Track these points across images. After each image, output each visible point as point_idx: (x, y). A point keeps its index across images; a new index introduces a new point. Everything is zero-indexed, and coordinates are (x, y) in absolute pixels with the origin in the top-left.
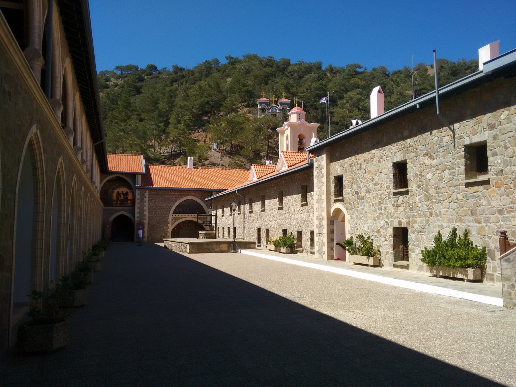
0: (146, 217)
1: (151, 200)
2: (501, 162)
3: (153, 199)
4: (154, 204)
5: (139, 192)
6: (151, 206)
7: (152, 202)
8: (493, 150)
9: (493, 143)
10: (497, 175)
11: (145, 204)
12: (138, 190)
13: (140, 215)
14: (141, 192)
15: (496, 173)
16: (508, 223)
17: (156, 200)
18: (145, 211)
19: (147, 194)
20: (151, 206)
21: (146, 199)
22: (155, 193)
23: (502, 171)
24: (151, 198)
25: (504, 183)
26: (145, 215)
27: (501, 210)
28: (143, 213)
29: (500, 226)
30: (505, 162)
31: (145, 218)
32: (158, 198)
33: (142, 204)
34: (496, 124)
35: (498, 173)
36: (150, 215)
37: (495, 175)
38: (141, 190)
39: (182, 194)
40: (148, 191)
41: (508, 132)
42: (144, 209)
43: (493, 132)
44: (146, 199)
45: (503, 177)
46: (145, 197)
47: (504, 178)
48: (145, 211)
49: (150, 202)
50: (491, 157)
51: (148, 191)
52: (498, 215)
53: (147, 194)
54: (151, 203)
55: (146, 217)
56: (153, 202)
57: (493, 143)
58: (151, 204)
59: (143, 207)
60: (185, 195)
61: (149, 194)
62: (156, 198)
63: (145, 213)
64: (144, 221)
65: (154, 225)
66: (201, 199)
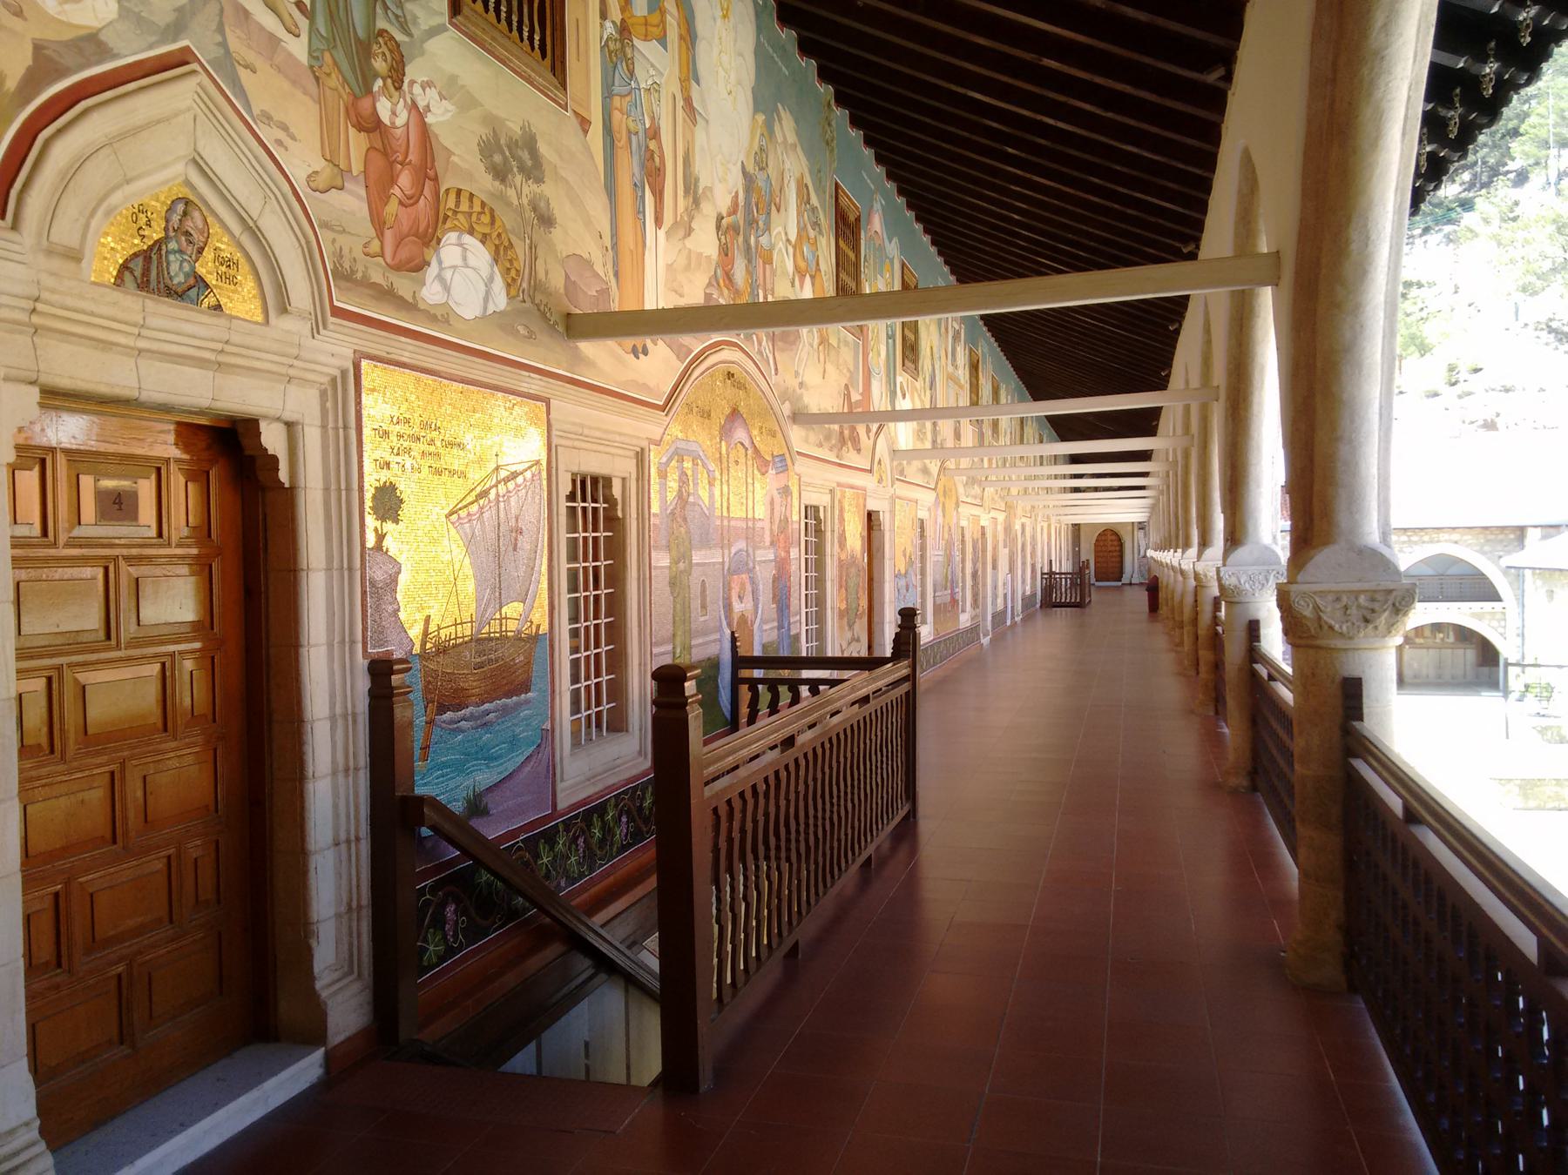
39: (1415, 538)
60: (1424, 542)
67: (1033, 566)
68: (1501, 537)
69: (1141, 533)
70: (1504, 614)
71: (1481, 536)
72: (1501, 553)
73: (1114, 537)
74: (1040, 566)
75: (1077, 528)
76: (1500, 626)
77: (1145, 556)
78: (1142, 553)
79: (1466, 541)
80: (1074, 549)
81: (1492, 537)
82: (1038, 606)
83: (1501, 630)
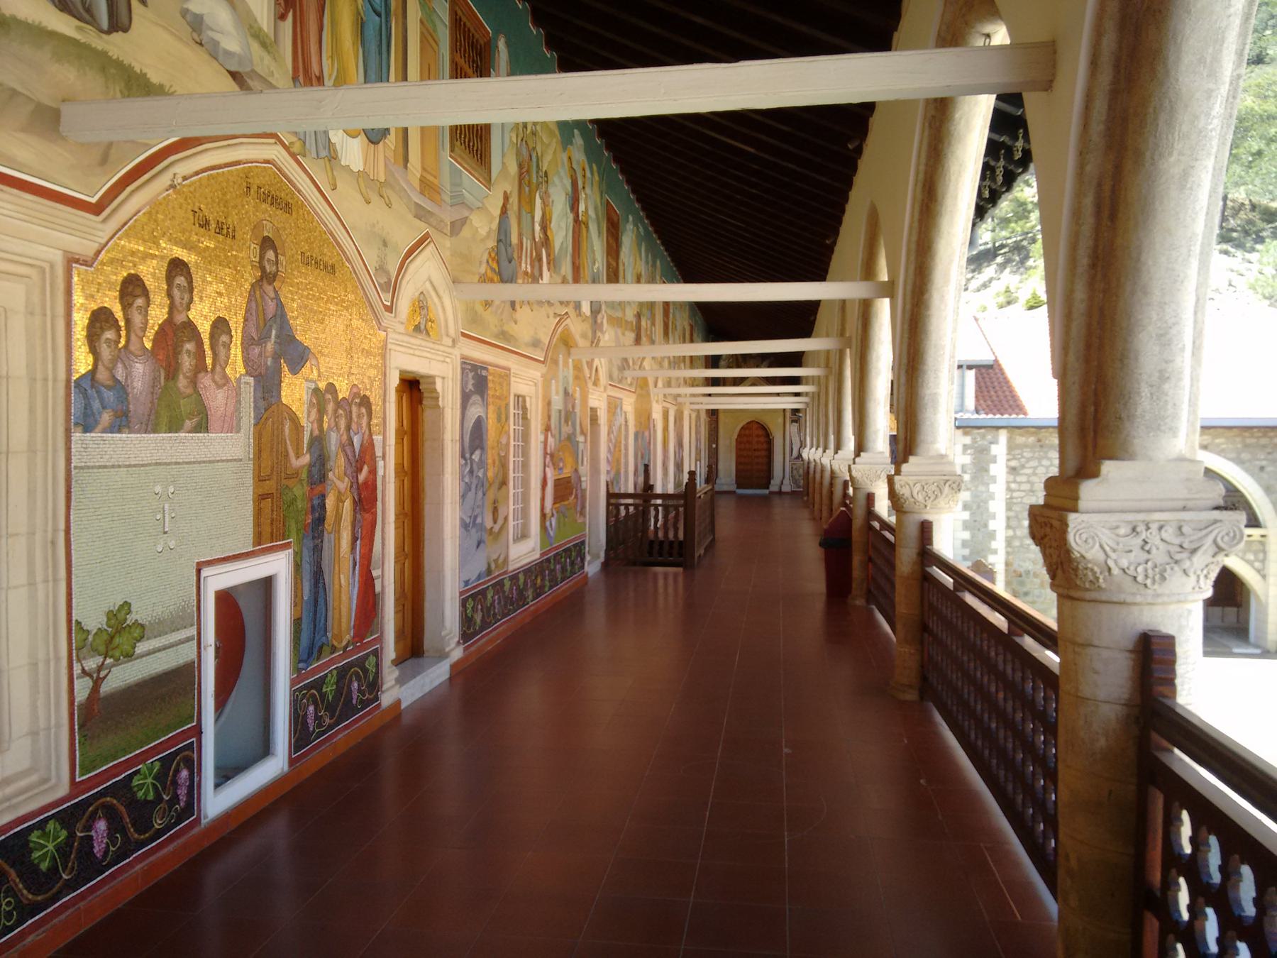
0: (999, 544)
1: (1013, 470)
3: (1023, 467)
4: (1026, 487)
5: (968, 440)
6: (1015, 494)
7: (1019, 479)
11: (992, 488)
12: (965, 434)
13: (973, 536)
14: (974, 440)
17: (1035, 468)
18: (993, 517)
19: (1000, 449)
20: (1015, 494)
21: (999, 470)
22: (1032, 439)
24: (1013, 463)
26: (992, 535)
28: (986, 526)
31: (994, 545)
32: (1045, 462)
33: (982, 488)
36: (1010, 533)
38: (976, 431)
40: (1003, 436)
42: (987, 509)
44: (999, 470)
46: (994, 460)
48: (993, 517)
49: (1011, 478)
51: (1003, 436)
53: (1000, 449)
54: (1015, 482)
55: (999, 544)
56: (1024, 479)
58: (1013, 486)
59: (986, 502)
61: (1011, 448)
62: (1034, 463)
63: (992, 525)
64: (991, 559)
65: (1028, 572)
66: (1239, 461)
67: (565, 490)
68: (1264, 441)
69: (795, 427)
70: (1262, 544)
71: (1238, 439)
72: (1264, 463)
73: (761, 432)
74: (603, 479)
75: (713, 414)
76: (1257, 560)
77: (800, 456)
78: (795, 453)
79: (1218, 445)
80: (710, 446)
81: (1253, 441)
82: (592, 567)
83: (1257, 565)
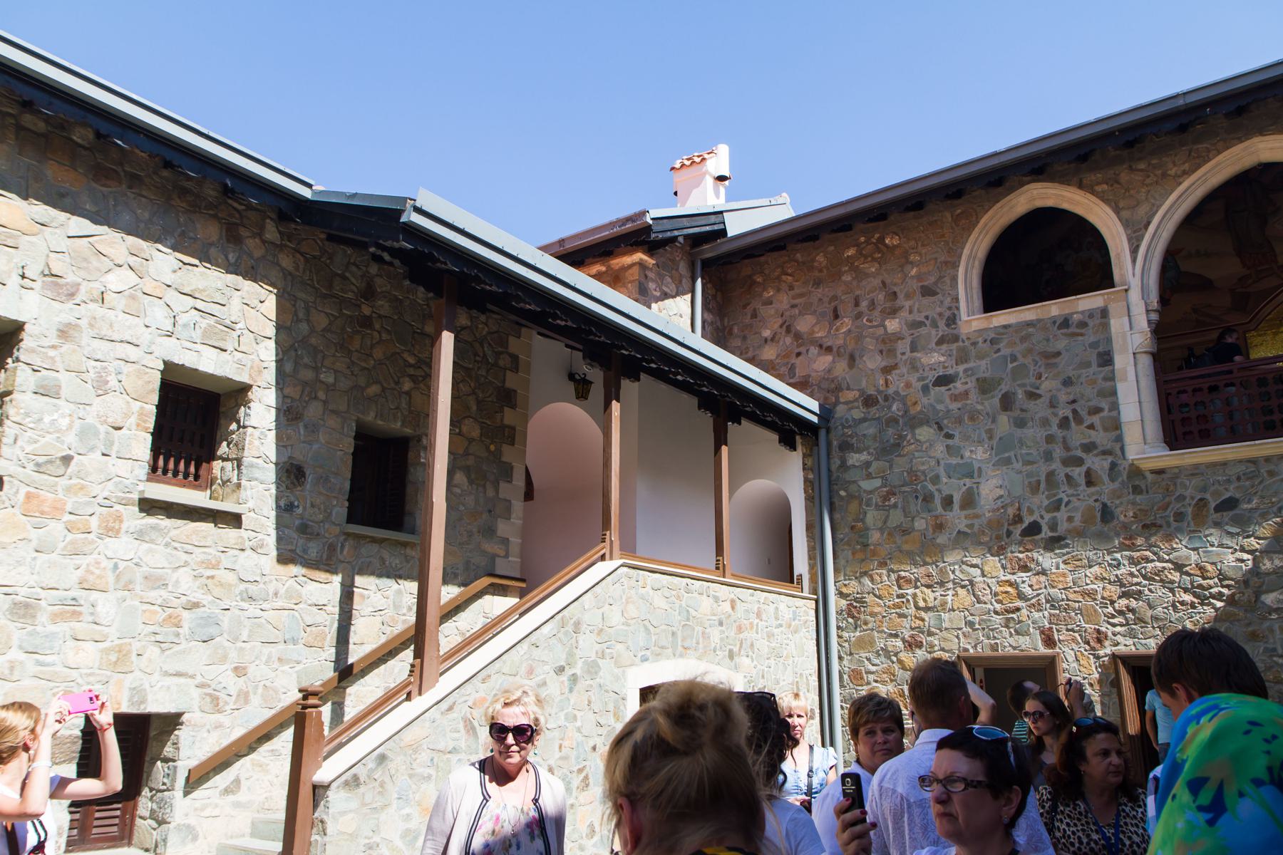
2: (70, 427)
8: (44, 372)
9: (53, 347)
10: (39, 469)
15: (41, 460)
16: (48, 659)
23: (67, 460)
25: (69, 508)
27: (27, 606)
29: (12, 669)
30: (86, 433)
34: (83, 289)
35: (50, 462)
37: (31, 466)
41: (122, 341)
43: (65, 313)
45: (63, 482)
47: (68, 489)
50: (30, 395)
52: (9, 623)
57: (53, 347)
